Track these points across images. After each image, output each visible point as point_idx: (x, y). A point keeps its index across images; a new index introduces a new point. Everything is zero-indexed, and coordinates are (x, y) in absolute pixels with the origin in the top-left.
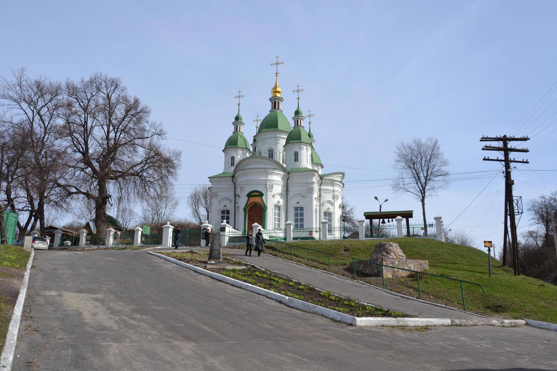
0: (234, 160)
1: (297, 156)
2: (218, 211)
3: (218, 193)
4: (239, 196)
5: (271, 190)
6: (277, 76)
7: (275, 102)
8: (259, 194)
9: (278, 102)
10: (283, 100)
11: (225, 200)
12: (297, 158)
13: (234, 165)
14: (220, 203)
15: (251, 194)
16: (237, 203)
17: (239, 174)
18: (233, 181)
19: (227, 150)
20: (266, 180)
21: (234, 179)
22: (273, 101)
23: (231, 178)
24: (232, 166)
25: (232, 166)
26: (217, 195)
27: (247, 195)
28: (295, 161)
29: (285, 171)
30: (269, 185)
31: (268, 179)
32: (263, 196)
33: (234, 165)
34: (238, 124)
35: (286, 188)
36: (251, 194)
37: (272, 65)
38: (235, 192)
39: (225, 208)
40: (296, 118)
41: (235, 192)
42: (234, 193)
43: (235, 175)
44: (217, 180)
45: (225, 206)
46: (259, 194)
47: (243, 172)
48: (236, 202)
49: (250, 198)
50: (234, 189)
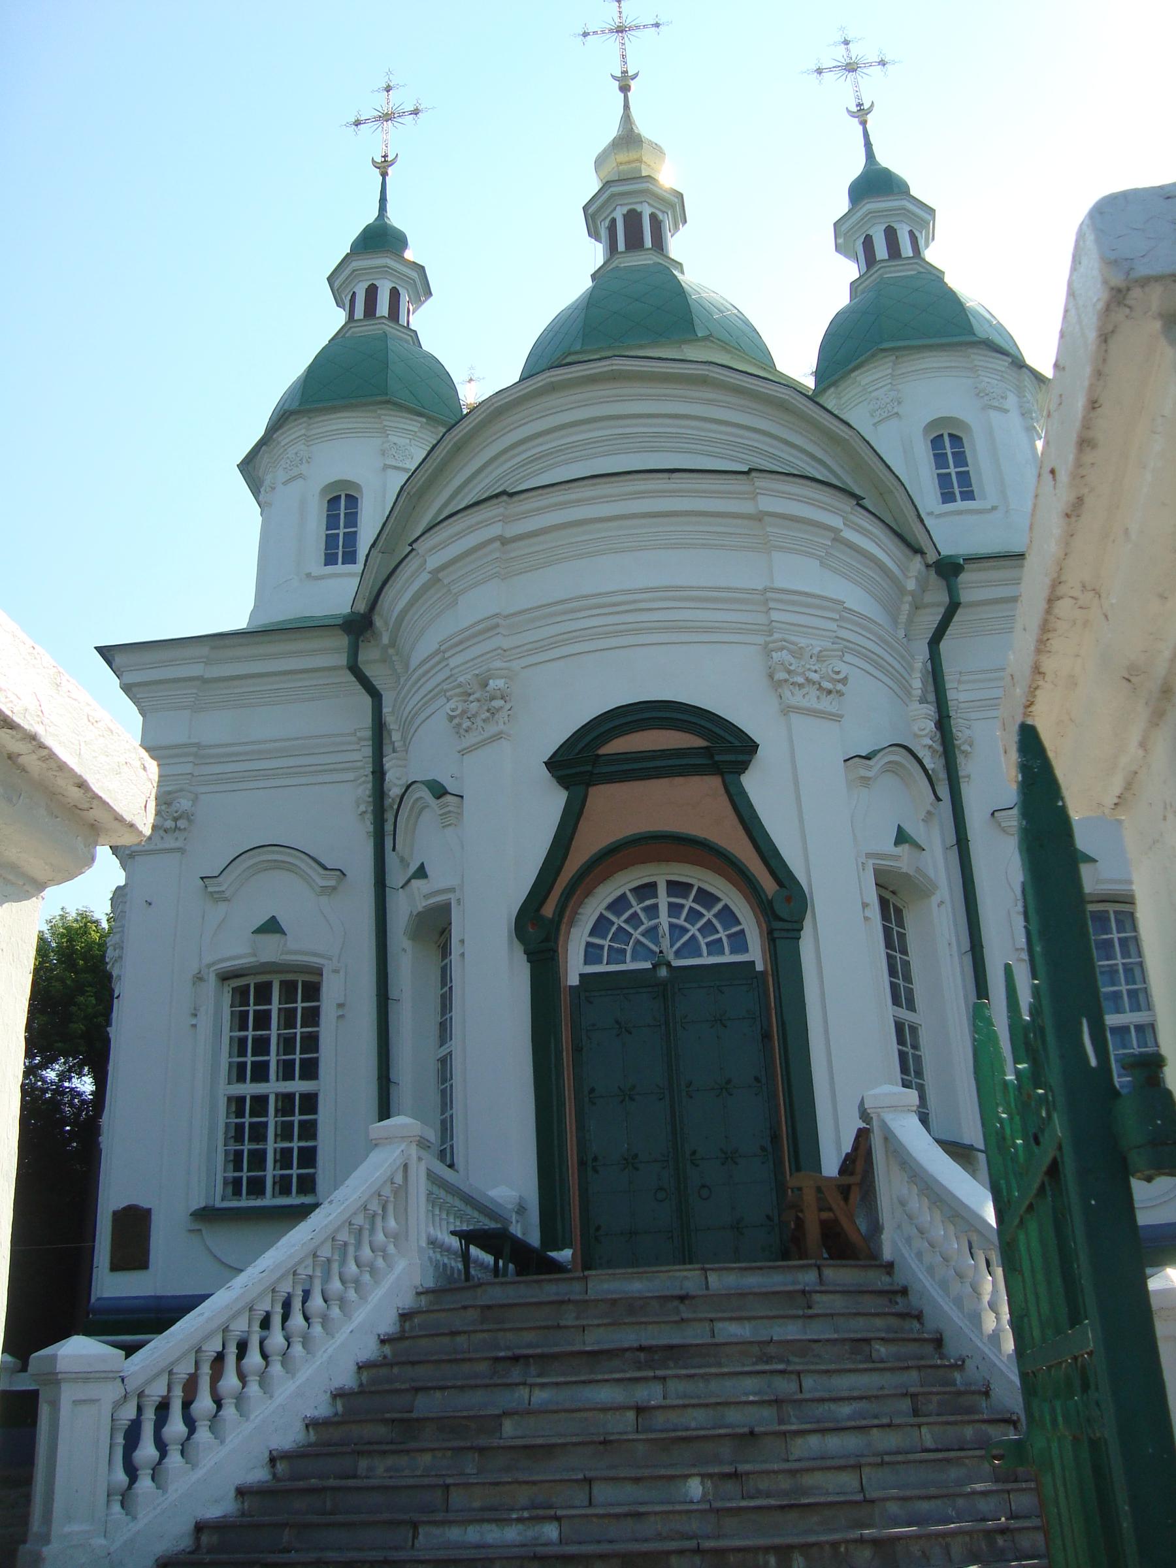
0: (352, 519)
1: (960, 458)
2: (199, 978)
3: (195, 800)
4: (439, 791)
5: (826, 704)
6: (625, 89)
7: (633, 219)
8: (699, 742)
9: (653, 217)
10: (685, 222)
11: (278, 865)
12: (964, 478)
13: (350, 558)
14: (218, 898)
15: (602, 751)
16: (421, 873)
17: (433, 562)
18: (355, 670)
19: (286, 437)
20: (767, 597)
21: (368, 656)
22: (619, 215)
23: (343, 641)
24: (330, 560)
25: (330, 560)
26: (187, 816)
27: (552, 764)
28: (948, 497)
29: (918, 551)
30: (798, 653)
31: (779, 583)
32: (743, 766)
33: (350, 558)
34: (385, 271)
35: (930, 709)
36: (602, 751)
37: (585, 34)
38: (379, 774)
39: (270, 950)
40: (874, 215)
41: (379, 774)
42: (365, 789)
43: (390, 592)
44: (196, 670)
45: (272, 926)
46: (699, 742)
47: (496, 530)
48: (396, 877)
49: (602, 797)
50: (368, 751)
